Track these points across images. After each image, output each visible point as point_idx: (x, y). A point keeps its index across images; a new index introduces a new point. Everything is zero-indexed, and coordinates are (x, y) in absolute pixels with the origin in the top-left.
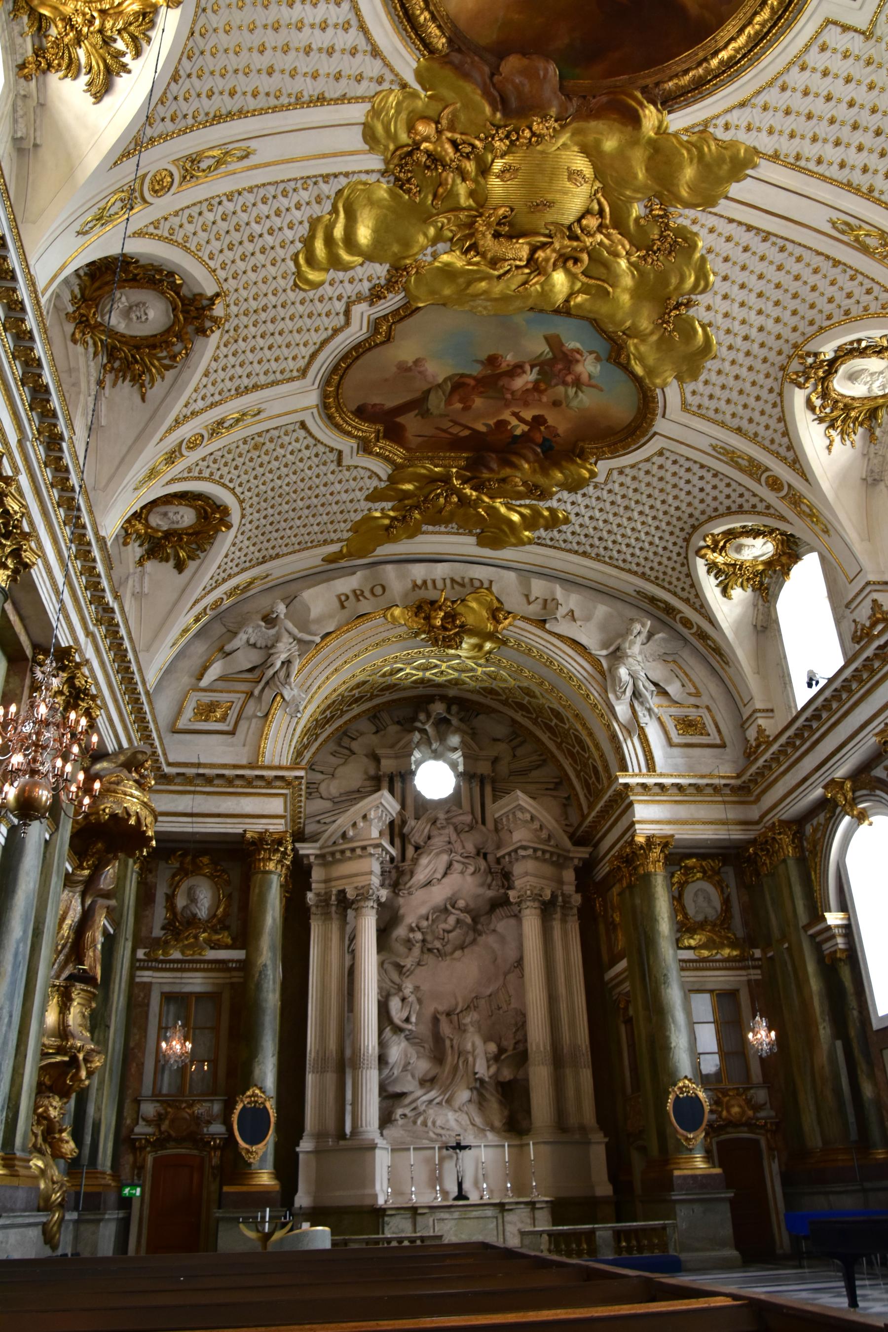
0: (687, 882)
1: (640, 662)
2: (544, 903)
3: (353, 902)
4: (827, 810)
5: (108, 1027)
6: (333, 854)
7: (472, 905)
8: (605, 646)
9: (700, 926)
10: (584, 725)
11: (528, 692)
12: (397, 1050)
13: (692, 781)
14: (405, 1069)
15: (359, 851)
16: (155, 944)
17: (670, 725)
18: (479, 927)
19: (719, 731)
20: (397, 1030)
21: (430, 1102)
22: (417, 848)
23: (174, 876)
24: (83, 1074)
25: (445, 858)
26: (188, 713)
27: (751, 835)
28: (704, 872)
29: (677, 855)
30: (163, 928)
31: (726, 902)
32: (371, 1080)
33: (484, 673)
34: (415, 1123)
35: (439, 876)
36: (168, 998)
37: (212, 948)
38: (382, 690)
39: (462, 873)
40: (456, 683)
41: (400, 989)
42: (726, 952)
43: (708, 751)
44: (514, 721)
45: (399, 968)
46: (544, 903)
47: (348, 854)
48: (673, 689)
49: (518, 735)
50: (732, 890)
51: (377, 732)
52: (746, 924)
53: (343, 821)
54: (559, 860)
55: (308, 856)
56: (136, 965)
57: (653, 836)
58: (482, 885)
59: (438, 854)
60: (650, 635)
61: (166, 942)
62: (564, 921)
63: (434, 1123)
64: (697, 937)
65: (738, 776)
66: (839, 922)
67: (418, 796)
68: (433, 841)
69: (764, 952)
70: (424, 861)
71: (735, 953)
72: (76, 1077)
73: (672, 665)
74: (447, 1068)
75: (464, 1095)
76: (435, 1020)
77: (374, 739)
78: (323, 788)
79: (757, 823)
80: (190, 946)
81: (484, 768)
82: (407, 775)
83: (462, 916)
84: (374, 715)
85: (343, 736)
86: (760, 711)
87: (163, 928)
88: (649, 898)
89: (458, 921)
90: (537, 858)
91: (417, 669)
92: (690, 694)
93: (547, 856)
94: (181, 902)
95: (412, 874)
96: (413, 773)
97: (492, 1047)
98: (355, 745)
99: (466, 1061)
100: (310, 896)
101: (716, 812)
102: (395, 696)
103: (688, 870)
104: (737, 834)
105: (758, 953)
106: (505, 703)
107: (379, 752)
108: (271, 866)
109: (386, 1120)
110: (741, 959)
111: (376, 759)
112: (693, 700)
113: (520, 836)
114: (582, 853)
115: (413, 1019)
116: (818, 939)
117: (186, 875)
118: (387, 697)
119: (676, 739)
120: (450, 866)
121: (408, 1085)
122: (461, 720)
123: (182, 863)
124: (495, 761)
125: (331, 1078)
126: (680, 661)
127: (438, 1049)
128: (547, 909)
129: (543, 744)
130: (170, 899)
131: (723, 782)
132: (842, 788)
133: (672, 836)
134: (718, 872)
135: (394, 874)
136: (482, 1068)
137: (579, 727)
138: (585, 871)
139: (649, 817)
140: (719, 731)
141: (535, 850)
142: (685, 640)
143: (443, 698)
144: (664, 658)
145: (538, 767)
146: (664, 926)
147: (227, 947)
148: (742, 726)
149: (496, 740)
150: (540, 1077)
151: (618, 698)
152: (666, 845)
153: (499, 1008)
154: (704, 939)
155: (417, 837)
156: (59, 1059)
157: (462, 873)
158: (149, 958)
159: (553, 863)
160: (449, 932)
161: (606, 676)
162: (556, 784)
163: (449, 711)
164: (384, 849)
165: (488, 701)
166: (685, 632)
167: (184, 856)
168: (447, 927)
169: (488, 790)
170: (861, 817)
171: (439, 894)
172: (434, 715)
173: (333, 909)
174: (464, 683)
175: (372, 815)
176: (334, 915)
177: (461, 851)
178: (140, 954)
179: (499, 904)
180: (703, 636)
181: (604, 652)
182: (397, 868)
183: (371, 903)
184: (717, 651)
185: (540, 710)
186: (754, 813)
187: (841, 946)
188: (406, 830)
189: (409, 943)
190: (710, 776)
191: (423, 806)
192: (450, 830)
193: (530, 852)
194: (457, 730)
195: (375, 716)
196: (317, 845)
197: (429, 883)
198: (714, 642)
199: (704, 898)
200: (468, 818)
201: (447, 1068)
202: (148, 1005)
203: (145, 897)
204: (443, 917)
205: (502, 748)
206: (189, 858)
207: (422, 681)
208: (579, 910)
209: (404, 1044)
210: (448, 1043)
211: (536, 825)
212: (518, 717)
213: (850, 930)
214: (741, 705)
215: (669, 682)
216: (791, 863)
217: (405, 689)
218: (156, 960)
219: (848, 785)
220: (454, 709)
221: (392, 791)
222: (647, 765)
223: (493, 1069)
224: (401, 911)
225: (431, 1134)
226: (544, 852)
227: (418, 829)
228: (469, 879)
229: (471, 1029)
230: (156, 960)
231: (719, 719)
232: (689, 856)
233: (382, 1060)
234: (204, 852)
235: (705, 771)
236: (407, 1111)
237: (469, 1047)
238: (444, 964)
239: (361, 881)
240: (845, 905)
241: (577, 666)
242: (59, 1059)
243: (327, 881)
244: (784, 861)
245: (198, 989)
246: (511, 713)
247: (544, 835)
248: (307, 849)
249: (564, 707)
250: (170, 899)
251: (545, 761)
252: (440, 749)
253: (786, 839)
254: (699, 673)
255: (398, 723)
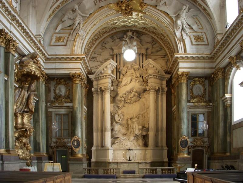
0: (194, 85)
1: (184, 20)
2: (156, 90)
3: (104, 91)
4: (229, 66)
5: (39, 122)
6: (98, 78)
7: (138, 91)
8: (175, 14)
9: (197, 97)
10: (169, 38)
11: (155, 28)
12: (117, 127)
13: (197, 56)
14: (119, 132)
15: (105, 77)
16: (52, 102)
17: (193, 39)
18: (141, 96)
19: (207, 40)
20: (117, 122)
21: (124, 139)
22: (123, 75)
23: (55, 85)
24: (29, 133)
25: (130, 78)
26: (54, 40)
27: (212, 72)
28: (200, 82)
29: (190, 78)
30: (54, 98)
31: (205, 90)
32: (108, 135)
33: (141, 23)
34: (120, 144)
35: (128, 83)
36: (56, 115)
37: (66, 103)
38: (112, 29)
39: (135, 82)
40: (134, 26)
41: (118, 112)
42: (202, 104)
43: (203, 46)
44: (152, 37)
45: (118, 107)
46: (156, 90)
47: (102, 77)
48: (195, 27)
49: (154, 42)
50: (207, 87)
51: (113, 41)
52: (209, 96)
53: (100, 69)
54: (161, 78)
55: (92, 78)
56: (46, 106)
57: (184, 72)
58: (141, 85)
59: (128, 77)
60: (189, 9)
61: (54, 102)
62: (162, 95)
63: (124, 145)
64: (195, 100)
65: (210, 54)
66: (229, 97)
67: (124, 60)
68: (128, 73)
69: (213, 104)
70: (124, 79)
71: (204, 104)
72: (27, 133)
73: (196, 20)
74: (129, 132)
75: (132, 138)
76: (127, 120)
77: (112, 44)
78: (98, 59)
79: (215, 68)
80: (60, 103)
81: (143, 52)
82: (121, 54)
83: (135, 94)
84: (112, 36)
85: (103, 43)
86: (218, 34)
87: (54, 98)
88: (181, 90)
89: (134, 95)
90: (154, 78)
91: (121, 22)
92: (200, 29)
93: (158, 77)
94: (57, 91)
95: (121, 82)
96: (123, 54)
97: (140, 127)
98: (106, 46)
99: (134, 130)
100: (93, 89)
101: (200, 65)
102: (117, 30)
103: (195, 81)
104: (208, 71)
105: (211, 104)
106: (149, 31)
107: (113, 47)
108: (77, 82)
109: (113, 143)
110: (207, 106)
111: (113, 50)
112: (200, 31)
113: (150, 71)
114: (169, 76)
115: (121, 120)
116: (224, 101)
117: (58, 84)
118: (114, 31)
119: (194, 43)
120: (132, 80)
121: (119, 135)
122: (137, 37)
123: (57, 82)
124: (147, 49)
125: (99, 134)
126: (198, 18)
127: (128, 127)
128: (157, 91)
129: (161, 44)
130: (55, 91)
131: (205, 56)
132: (233, 59)
133: (189, 72)
134: (204, 82)
135: (117, 83)
136: (137, 132)
137: (168, 39)
138: (169, 82)
139: (184, 67)
140: (207, 40)
141: (154, 76)
142: (200, 11)
143: (131, 31)
144: (193, 17)
145: (160, 51)
146: (184, 97)
147: (69, 103)
148: (214, 38)
149: (147, 43)
150: (151, 134)
151: (177, 30)
152: (187, 75)
153: (145, 117)
154: (197, 100)
155: (123, 72)
156: (22, 130)
157: (135, 82)
158: (51, 106)
159: (159, 79)
160: (132, 98)
161: (174, 24)
162: (164, 56)
163: (133, 35)
164: (111, 76)
165: (144, 31)
166: (200, 8)
167: (57, 79)
168: (131, 97)
169: (144, 58)
170: (238, 67)
171: (128, 88)
172: (128, 36)
173: (99, 92)
174: (137, 26)
175: (108, 66)
176: (99, 94)
177: (135, 76)
178: (48, 104)
179: (145, 91)
180: (205, 10)
181: (174, 16)
182: (118, 81)
183: (108, 91)
184: (209, 14)
185: (158, 33)
186: (214, 65)
187: (229, 103)
188: (120, 70)
189: (120, 101)
190: (202, 54)
191: (125, 63)
192: (133, 69)
193: (152, 76)
194: (136, 40)
195: (112, 37)
196: (94, 75)
197: (126, 85)
198: (208, 11)
199: (198, 89)
200: (138, 66)
201: (129, 132)
202: (52, 117)
203: (48, 90)
204: (130, 94)
205: (149, 45)
206: (58, 80)
207: (124, 26)
208: (167, 92)
209: (119, 126)
210: (130, 126)
211: (155, 68)
212: (153, 36)
213: (231, 99)
214: (215, 32)
215: (193, 25)
216: (221, 80)
217: (119, 28)
218: (52, 106)
219: (235, 58)
220: (135, 34)
221: (113, 59)
222: (184, 51)
223: (140, 132)
224: (118, 93)
225: (124, 147)
226: (156, 76)
227: (123, 70)
228: (137, 84)
229: (135, 123)
230: (52, 106)
231: (208, 36)
232: (196, 77)
233: (112, 130)
234: (62, 78)
235: (201, 52)
236: (118, 142)
237: (134, 127)
238: (130, 106)
239: (105, 85)
240: (231, 93)
241: (166, 20)
242: (22, 130)
243: (97, 85)
244: (219, 79)
245: (63, 113)
246: (151, 34)
247: (157, 71)
248: (91, 76)
249: (164, 33)
250: (55, 91)
251: (161, 49)
252: (131, 46)
253: (220, 73)
254: (203, 21)
255: (119, 38)
